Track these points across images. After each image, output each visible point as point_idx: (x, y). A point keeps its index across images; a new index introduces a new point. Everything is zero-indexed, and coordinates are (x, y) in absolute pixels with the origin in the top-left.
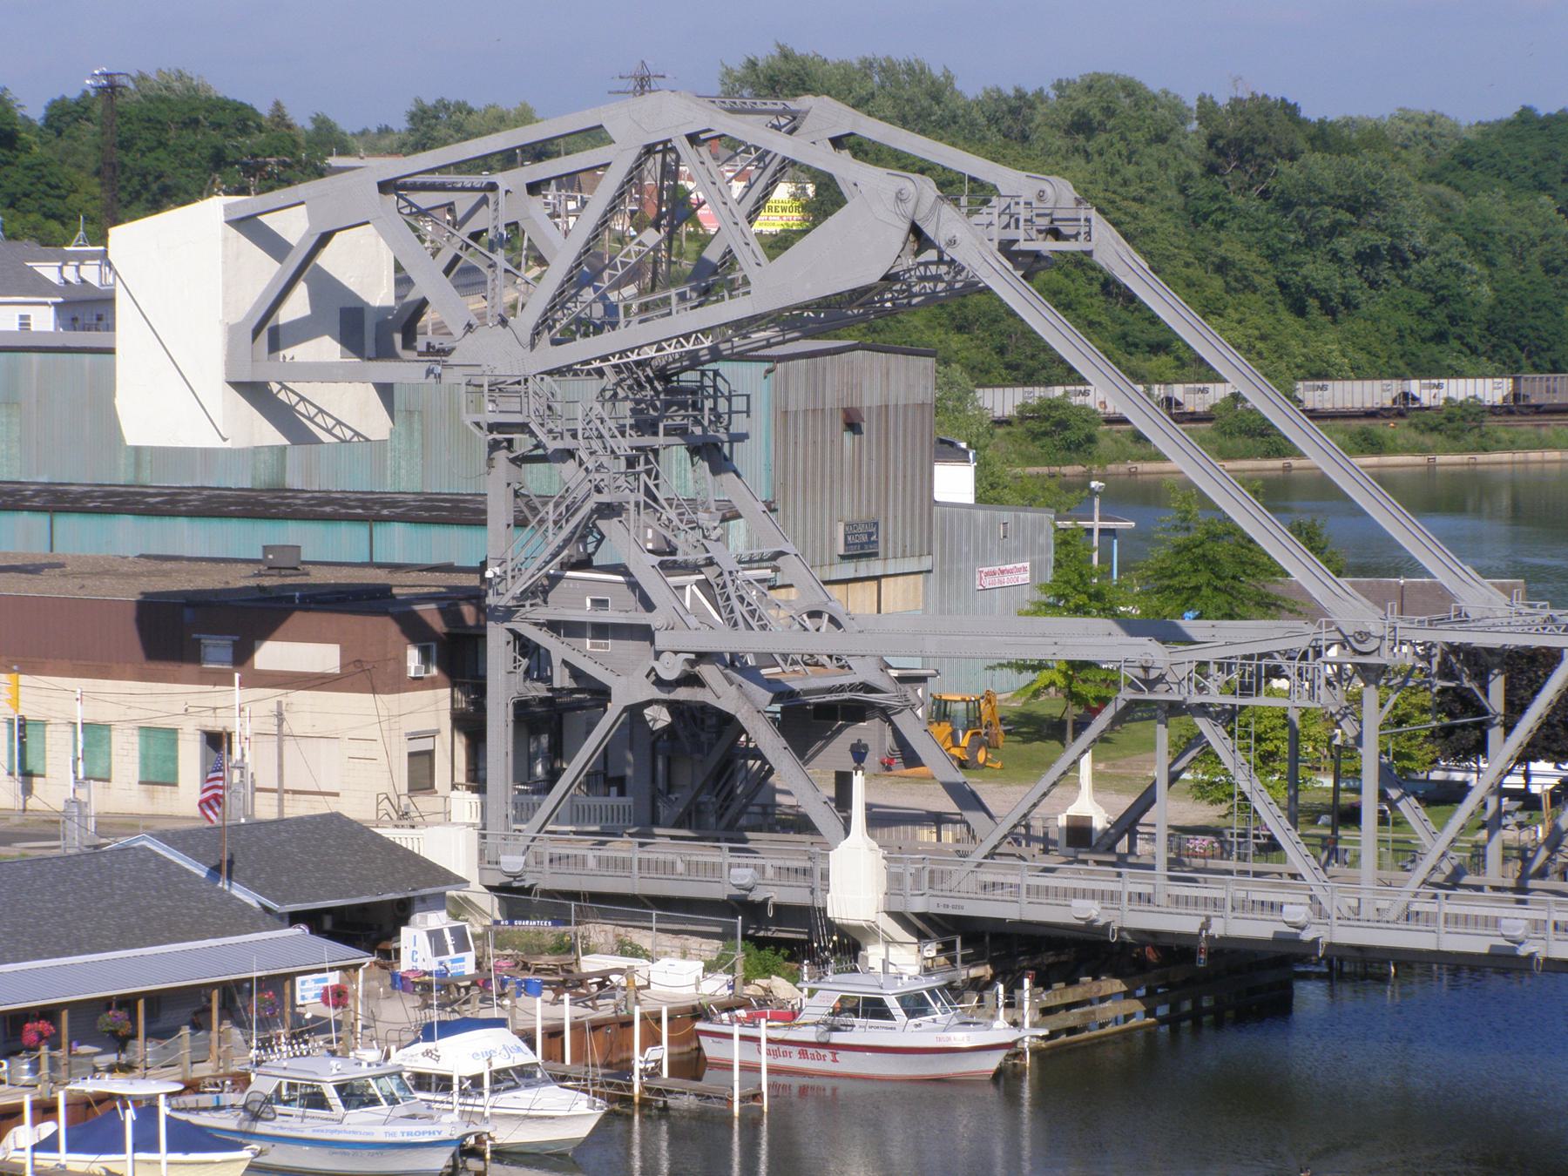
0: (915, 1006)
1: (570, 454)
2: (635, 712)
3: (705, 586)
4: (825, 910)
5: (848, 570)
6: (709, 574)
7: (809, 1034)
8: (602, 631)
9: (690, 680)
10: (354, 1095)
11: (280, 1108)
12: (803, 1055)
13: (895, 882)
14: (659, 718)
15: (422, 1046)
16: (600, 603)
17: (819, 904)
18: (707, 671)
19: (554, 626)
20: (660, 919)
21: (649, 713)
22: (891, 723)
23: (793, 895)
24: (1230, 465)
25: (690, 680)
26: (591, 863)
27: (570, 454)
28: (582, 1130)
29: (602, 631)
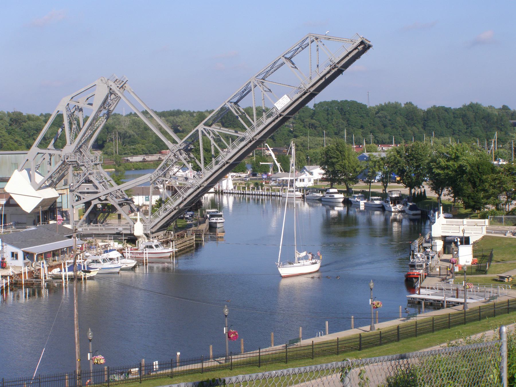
0: (157, 246)
1: (83, 165)
2: (96, 206)
3: (103, 185)
4: (133, 234)
5: (64, 187)
6: (103, 183)
7: (141, 252)
8: (88, 193)
9: (106, 200)
10: (104, 261)
11: (92, 264)
12: (140, 255)
13: (145, 229)
14: (99, 206)
15: (106, 254)
16: (88, 189)
17: (132, 233)
18: (108, 198)
19: (80, 193)
20: (109, 236)
21: (98, 205)
22: (130, 206)
23: (128, 232)
24: (106, 170)
25: (106, 200)
26: (88, 229)
27: (83, 165)
28: (133, 265)
29: (88, 193)
